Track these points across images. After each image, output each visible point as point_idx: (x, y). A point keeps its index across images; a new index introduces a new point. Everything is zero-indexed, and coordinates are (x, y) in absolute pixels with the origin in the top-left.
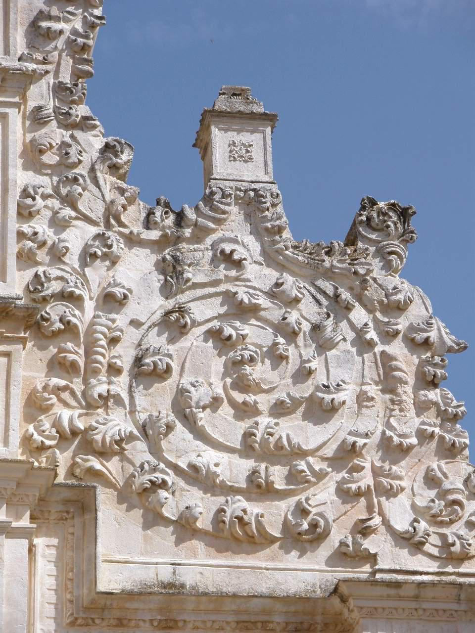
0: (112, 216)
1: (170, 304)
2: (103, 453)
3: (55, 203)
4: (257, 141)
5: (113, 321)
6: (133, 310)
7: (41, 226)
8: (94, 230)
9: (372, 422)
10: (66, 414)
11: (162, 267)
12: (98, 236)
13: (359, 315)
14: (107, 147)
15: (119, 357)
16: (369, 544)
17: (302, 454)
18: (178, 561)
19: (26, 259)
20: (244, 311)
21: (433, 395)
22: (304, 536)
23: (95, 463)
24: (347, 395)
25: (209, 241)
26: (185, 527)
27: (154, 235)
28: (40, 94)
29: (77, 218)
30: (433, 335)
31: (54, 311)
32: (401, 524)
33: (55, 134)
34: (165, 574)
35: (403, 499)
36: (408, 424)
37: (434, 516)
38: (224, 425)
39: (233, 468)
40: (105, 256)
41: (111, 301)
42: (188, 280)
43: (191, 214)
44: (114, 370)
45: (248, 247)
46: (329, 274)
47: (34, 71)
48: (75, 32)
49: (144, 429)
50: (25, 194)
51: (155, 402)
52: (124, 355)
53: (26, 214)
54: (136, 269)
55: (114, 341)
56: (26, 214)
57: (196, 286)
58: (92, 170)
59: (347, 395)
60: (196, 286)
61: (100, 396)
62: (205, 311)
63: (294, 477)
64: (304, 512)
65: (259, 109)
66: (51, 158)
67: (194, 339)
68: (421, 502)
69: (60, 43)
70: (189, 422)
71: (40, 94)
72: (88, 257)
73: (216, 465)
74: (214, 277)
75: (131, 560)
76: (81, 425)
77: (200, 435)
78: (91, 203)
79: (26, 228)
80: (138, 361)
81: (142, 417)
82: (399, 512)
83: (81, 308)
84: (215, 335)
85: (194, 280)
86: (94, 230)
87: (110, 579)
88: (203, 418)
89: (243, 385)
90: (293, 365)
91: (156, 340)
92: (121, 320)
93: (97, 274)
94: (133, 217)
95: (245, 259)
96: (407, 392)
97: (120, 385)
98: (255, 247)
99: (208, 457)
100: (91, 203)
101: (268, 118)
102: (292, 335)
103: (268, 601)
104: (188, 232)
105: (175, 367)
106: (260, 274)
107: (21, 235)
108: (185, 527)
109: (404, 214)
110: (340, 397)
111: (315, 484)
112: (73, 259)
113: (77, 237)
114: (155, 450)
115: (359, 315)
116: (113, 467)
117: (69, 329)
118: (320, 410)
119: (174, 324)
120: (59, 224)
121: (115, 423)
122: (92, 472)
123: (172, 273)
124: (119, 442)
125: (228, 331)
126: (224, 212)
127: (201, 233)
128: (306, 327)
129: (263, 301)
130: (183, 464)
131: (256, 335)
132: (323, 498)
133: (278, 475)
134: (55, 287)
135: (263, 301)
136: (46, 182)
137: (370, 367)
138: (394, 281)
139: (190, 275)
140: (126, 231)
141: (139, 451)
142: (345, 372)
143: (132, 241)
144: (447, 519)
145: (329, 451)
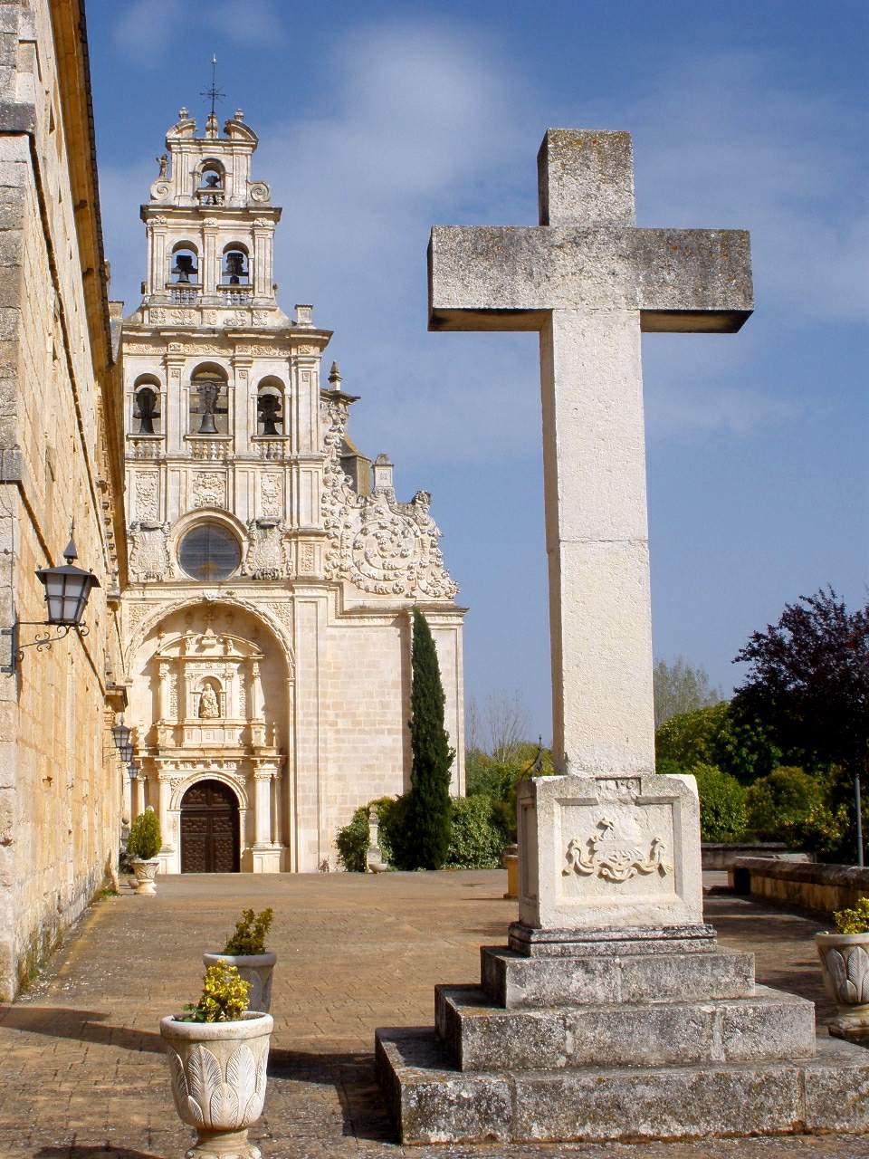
1: (363, 527)
3: (332, 498)
4: (387, 471)
6: (353, 529)
7: (328, 505)
8: (342, 505)
9: (417, 559)
11: (361, 515)
13: (415, 527)
14: (346, 480)
16: (414, 593)
19: (324, 515)
21: (434, 550)
22: (397, 591)
24: (410, 552)
25: (374, 506)
26: (367, 590)
27: (359, 506)
30: (435, 533)
31: (331, 531)
32: (424, 588)
33: (332, 476)
34: (361, 604)
35: (424, 581)
36: (426, 560)
38: (377, 561)
39: (379, 573)
43: (369, 499)
44: (348, 547)
45: (385, 507)
49: (355, 564)
51: (359, 555)
52: (350, 543)
54: (354, 515)
62: (373, 528)
64: (397, 586)
65: (389, 463)
66: (330, 484)
67: (370, 536)
68: (429, 582)
69: (332, 445)
70: (368, 561)
71: (327, 463)
76: (339, 564)
77: (371, 565)
78: (341, 497)
80: (354, 545)
81: (355, 561)
82: (423, 584)
84: (375, 535)
86: (342, 505)
87: (346, 608)
88: (371, 560)
89: (382, 549)
90: (395, 544)
91: (360, 537)
93: (343, 519)
94: (353, 500)
96: (428, 548)
97: (349, 551)
98: (386, 506)
99: (374, 572)
100: (341, 497)
101: (390, 465)
102: (396, 535)
104: (368, 504)
105: (364, 545)
106: (388, 516)
108: (367, 590)
109: (429, 495)
110: (407, 553)
112: (337, 515)
113: (337, 509)
114: (359, 570)
115: (415, 527)
117: (336, 537)
118: (403, 556)
119: (364, 532)
121: (348, 563)
122: (342, 577)
123: (363, 516)
127: (371, 504)
129: (389, 525)
131: (384, 533)
132: (403, 582)
133: (390, 574)
134: (331, 525)
135: (389, 525)
136: (328, 491)
138: (425, 516)
141: (355, 570)
142: (410, 545)
143: (352, 507)
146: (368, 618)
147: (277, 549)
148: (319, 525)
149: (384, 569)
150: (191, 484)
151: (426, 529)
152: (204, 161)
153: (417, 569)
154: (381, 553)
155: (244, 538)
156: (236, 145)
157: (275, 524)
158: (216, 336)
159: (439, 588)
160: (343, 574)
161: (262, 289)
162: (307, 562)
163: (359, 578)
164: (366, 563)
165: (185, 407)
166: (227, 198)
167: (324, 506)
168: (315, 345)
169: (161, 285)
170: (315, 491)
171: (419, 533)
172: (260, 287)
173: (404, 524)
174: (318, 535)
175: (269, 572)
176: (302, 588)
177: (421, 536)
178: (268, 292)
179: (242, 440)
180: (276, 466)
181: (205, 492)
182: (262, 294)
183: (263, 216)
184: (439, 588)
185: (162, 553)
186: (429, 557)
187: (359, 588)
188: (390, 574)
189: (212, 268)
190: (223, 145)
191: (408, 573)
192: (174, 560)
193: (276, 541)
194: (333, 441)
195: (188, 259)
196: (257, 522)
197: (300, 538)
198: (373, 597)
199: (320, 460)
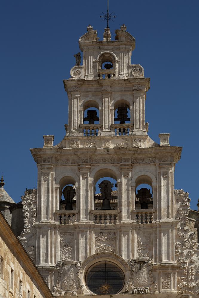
0: (191, 248)
5: (192, 266)
8: (188, 250)
10: (184, 283)
12: (189, 252)
15: (193, 272)
28: (179, 226)
41: (192, 263)
44: (192, 275)
48: (185, 213)
50: (177, 245)
53: (177, 248)
56: (177, 248)
58: (188, 239)
61: (190, 279)
71: (179, 226)
72: (187, 255)
79: (177, 251)
83: (186, 264)
86: (188, 250)
92: (193, 266)
107: (176, 252)
113: (185, 252)
140: (194, 250)
148: (174, 262)
157: (146, 261)
161: (138, 126)
162: (167, 284)
165: (91, 194)
166: (117, 75)
169: (76, 126)
170: (170, 241)
172: (137, 125)
174: (173, 267)
175: (142, 290)
178: (141, 128)
179: (125, 218)
182: (139, 130)
189: (108, 116)
192: (83, 283)
195: (94, 112)
196: (135, 260)
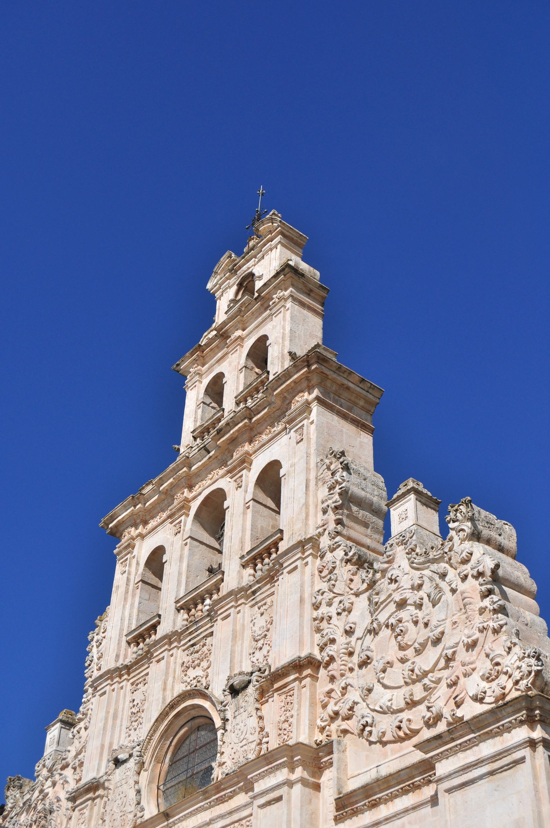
2: (348, 718)
6: (359, 633)
13: (452, 574)
17: (425, 674)
18: (379, 764)
20: (402, 604)
23: (345, 725)
27: (365, 586)
29: (335, 597)
37: (488, 678)
40: (344, 610)
42: (377, 603)
46: (434, 561)
47: (319, 533)
55: (351, 654)
56: (316, 607)
57: (382, 603)
59: (447, 627)
60: (382, 603)
63: (426, 688)
67: (385, 633)
73: (389, 701)
74: (388, 594)
75: (361, 772)
77: (385, 687)
85: (380, 601)
92: (353, 639)
95: (398, 576)
103: (408, 770)
104: (378, 575)
111: (435, 688)
116: (353, 725)
120: (330, 604)
124: (351, 709)
125: (392, 621)
126: (390, 556)
128: (426, 599)
130: (378, 708)
133: (418, 691)
136: (324, 586)
137: (455, 604)
139: (376, 600)
143: (357, 595)
144: (494, 677)
145: (442, 663)
146: (386, 801)
147: (253, 722)
148: (310, 648)
149: (406, 683)
150: (179, 669)
151: (467, 568)
152: (240, 285)
153: (462, 655)
154: (401, 654)
155: (218, 723)
156: (265, 245)
158: (212, 453)
159: (503, 679)
160: (345, 725)
162: (286, 725)
163: (363, 722)
164: (378, 688)
167: (315, 614)
168: (310, 390)
171: (457, 583)
173: (431, 579)
176: (262, 776)
177: (461, 587)
180: (268, 586)
181: (192, 673)
183: (277, 288)
184: (503, 679)
185: (132, 794)
186: (478, 621)
187: (371, 743)
188: (418, 691)
190: (255, 257)
191: (445, 673)
193: (251, 709)
194: (330, 502)
197: (276, 686)
198: (393, 752)
199: (313, 541)
